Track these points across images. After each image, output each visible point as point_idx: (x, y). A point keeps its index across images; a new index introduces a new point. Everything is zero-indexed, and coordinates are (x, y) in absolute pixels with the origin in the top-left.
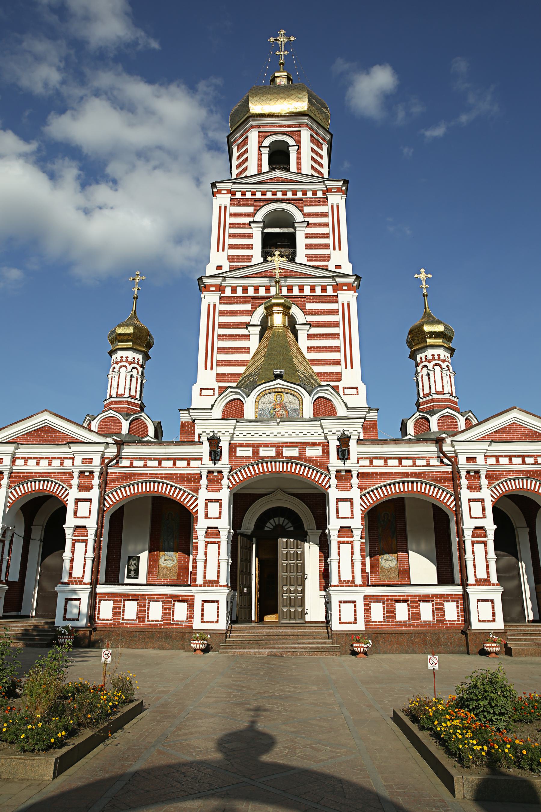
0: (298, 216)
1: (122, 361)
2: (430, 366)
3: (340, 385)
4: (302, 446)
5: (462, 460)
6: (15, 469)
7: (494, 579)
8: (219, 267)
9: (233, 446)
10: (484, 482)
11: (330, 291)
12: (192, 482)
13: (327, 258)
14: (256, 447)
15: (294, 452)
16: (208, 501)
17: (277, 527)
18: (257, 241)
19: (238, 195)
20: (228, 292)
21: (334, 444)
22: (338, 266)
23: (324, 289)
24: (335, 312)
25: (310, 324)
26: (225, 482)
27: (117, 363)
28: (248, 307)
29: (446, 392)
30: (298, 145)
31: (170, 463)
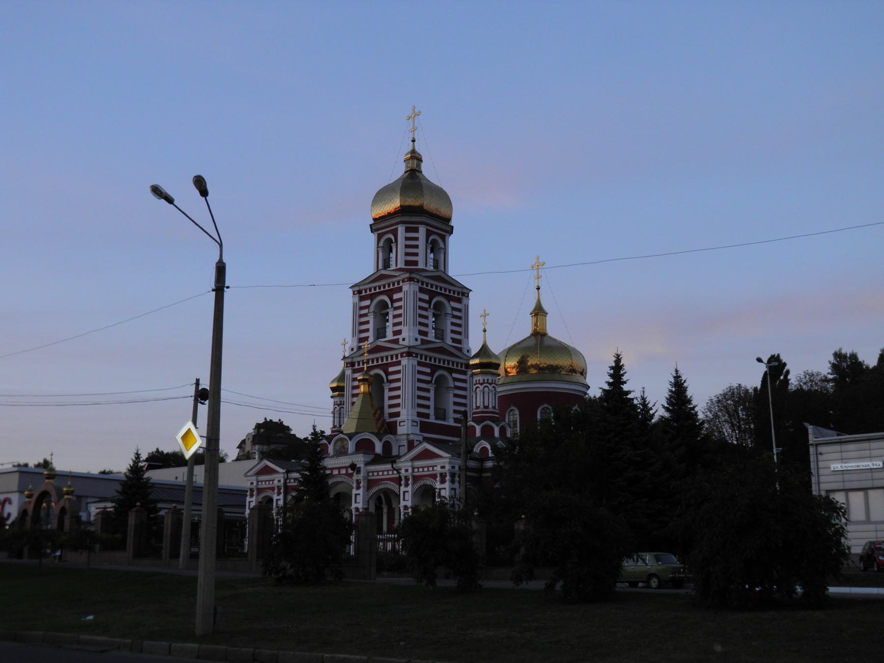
5: (403, 471)
6: (260, 486)
10: (410, 482)
14: (332, 469)
15: (343, 471)
19: (364, 294)
22: (404, 339)
23: (397, 356)
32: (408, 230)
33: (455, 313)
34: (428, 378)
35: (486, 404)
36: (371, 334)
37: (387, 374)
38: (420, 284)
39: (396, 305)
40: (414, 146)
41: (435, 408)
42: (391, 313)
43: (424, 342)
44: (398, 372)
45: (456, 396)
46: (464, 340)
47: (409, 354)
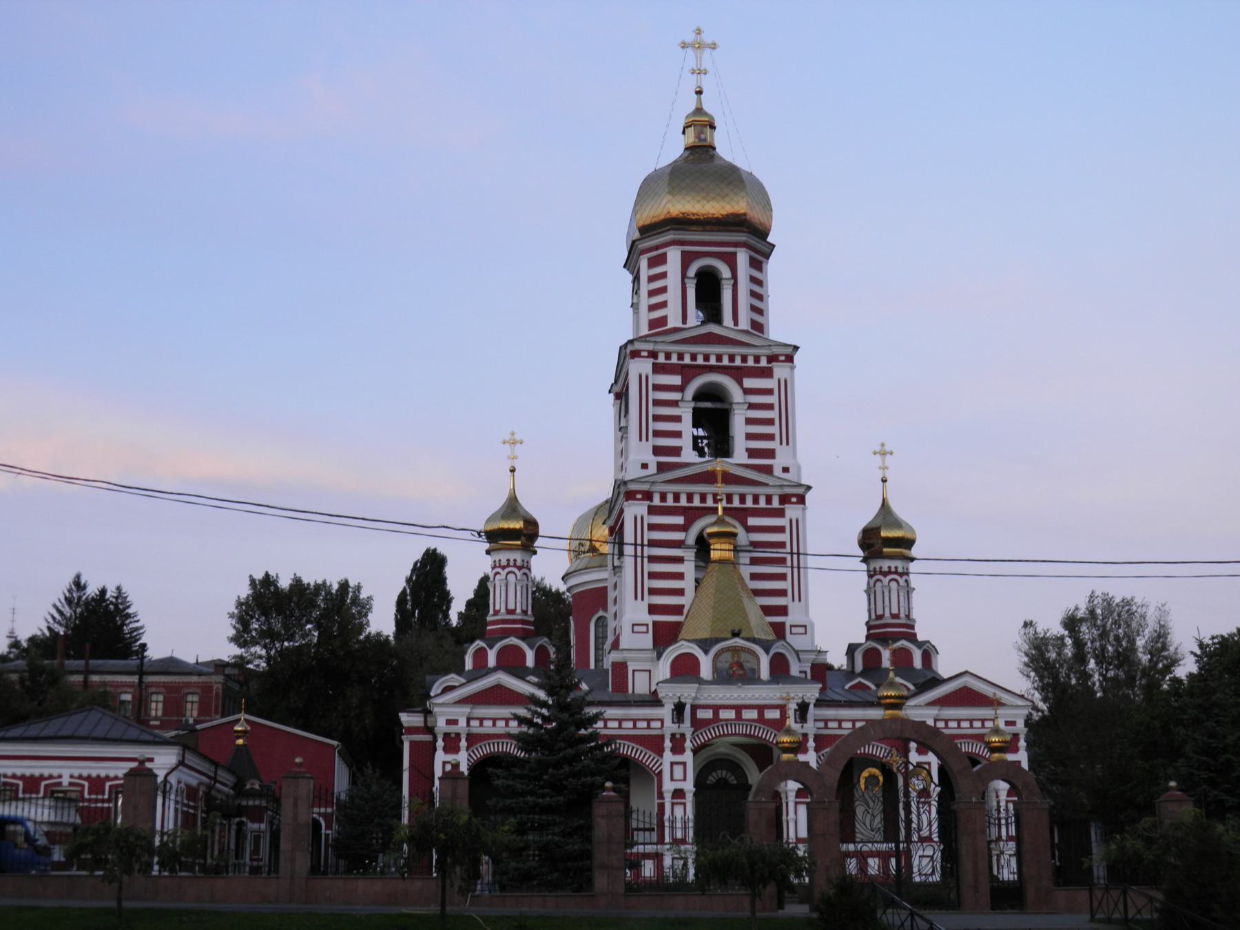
0: (736, 394)
1: (508, 565)
2: (886, 580)
3: (789, 620)
4: (761, 709)
7: (935, 837)
8: (645, 466)
9: (694, 708)
11: (776, 503)
12: (655, 744)
13: (770, 454)
14: (716, 709)
15: (753, 714)
16: (672, 764)
17: (719, 780)
18: (687, 427)
19: (661, 359)
20: (656, 501)
21: (792, 706)
22: (786, 470)
23: (769, 499)
24: (781, 529)
25: (755, 545)
26: (688, 744)
27: (503, 568)
28: (679, 520)
29: (902, 615)
31: (630, 724)
37: (749, 529)
40: (700, 101)
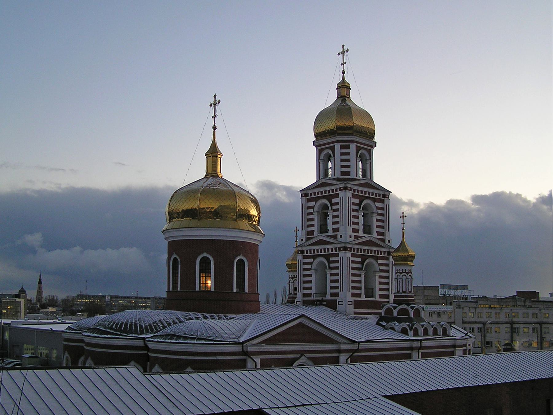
28: (311, 260)
30: (334, 156)
32: (342, 147)
33: (379, 211)
34: (359, 266)
35: (404, 290)
36: (316, 229)
38: (352, 192)
39: (335, 207)
41: (366, 288)
42: (331, 214)
43: (356, 237)
44: (337, 262)
45: (380, 277)
46: (387, 234)
47: (345, 249)
